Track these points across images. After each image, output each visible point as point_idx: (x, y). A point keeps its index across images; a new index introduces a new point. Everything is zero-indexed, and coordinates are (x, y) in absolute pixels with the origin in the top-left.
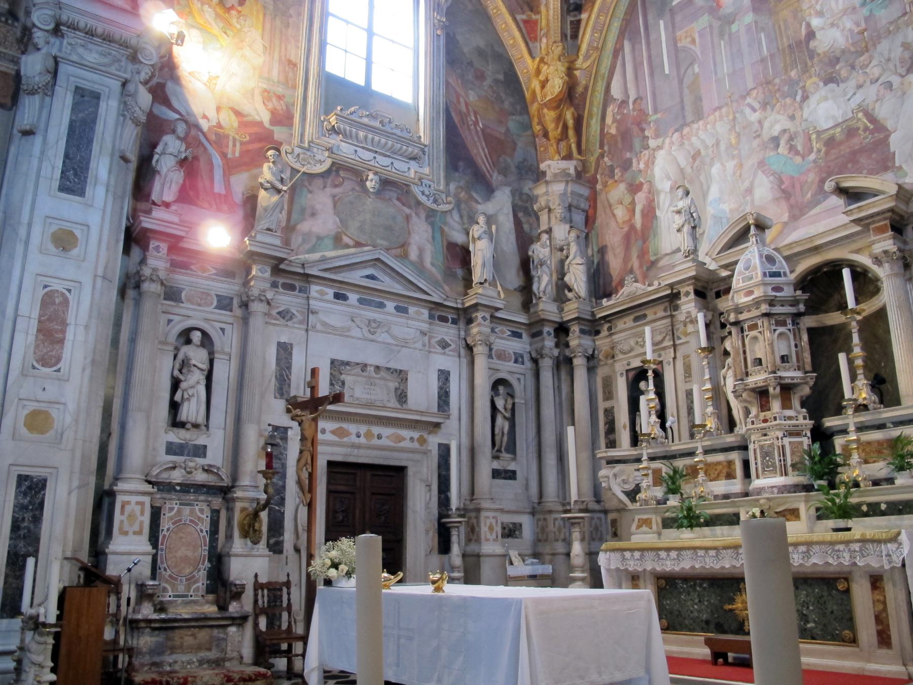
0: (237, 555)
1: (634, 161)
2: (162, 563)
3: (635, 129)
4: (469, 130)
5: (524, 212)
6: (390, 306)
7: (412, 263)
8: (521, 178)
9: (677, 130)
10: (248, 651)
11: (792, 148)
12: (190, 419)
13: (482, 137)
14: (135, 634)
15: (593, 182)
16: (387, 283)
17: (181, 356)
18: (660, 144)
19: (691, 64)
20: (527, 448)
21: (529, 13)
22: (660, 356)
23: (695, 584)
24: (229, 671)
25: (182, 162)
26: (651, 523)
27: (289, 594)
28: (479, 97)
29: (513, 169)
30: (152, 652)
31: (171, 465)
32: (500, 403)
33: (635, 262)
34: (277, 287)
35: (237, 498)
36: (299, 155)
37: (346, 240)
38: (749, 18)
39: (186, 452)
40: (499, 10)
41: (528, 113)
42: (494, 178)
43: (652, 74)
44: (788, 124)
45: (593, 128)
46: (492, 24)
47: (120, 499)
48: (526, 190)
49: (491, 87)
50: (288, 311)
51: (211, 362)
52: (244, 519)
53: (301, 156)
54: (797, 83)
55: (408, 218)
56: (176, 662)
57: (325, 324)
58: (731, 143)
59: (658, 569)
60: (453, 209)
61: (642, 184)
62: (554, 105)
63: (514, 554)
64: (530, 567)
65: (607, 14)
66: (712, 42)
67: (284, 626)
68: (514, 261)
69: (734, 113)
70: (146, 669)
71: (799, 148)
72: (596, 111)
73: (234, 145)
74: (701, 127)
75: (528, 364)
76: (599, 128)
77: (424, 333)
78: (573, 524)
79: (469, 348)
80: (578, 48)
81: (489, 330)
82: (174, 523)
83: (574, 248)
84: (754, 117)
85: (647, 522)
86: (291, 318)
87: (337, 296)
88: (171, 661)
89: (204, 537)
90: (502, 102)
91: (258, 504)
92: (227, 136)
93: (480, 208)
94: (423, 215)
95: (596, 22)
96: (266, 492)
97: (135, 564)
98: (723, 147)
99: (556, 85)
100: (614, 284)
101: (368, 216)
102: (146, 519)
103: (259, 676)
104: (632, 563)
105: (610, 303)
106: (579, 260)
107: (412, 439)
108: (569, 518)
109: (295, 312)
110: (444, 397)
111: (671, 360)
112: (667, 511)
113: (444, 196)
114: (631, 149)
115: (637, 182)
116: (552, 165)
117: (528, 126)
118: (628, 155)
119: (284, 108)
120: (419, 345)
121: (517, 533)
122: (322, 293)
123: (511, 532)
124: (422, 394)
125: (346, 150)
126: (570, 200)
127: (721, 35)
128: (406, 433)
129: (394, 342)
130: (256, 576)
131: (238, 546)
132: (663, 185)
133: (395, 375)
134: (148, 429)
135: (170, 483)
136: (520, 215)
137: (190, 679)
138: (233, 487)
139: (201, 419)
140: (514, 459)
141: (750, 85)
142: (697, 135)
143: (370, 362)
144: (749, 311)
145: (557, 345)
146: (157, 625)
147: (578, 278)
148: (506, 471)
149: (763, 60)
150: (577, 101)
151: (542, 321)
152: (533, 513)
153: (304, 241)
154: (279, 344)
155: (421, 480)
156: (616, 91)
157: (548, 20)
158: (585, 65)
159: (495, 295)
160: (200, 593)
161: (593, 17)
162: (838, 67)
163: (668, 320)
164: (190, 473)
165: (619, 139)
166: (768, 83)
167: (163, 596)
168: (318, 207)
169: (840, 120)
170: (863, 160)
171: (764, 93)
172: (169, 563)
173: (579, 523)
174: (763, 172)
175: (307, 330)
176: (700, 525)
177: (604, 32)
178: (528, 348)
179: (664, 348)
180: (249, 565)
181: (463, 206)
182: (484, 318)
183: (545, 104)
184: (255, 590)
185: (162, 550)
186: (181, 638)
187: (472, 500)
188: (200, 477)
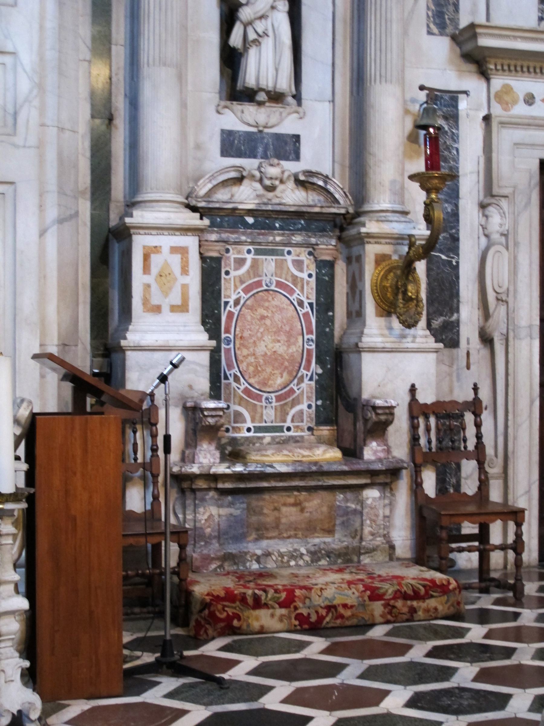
0: (373, 350)
2: (230, 366)
10: (402, 535)
12: (263, 84)
14: (189, 502)
24: (371, 576)
27: (478, 425)
30: (221, 535)
31: (233, 174)
35: (369, 235)
39: (260, 150)
52: (385, 277)
67: (470, 487)
70: (213, 566)
82: (246, 290)
88: (259, 552)
89: (306, 315)
91: (411, 245)
97: (175, 366)
102: (193, 281)
103: (432, 588)
130: (413, 390)
131: (375, 331)
134: (183, 105)
135: (235, 209)
138: (358, 214)
146: (228, 485)
160: (305, 425)
167: (238, 430)
180: (397, 368)
184: (413, 417)
185: (228, 342)
186: (275, 509)
188: (292, 197)
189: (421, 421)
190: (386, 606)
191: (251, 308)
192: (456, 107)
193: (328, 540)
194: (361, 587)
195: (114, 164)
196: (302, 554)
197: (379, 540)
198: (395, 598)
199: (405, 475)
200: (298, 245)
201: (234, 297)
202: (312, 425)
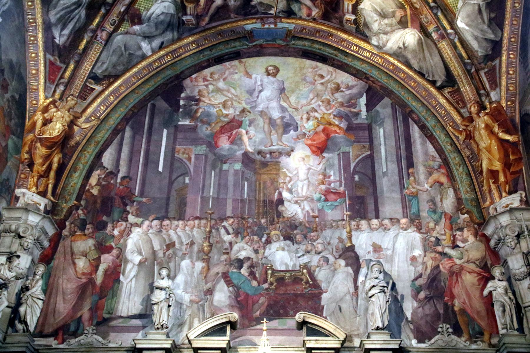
1: (110, 226)
3: (118, 201)
9: (157, 218)
11: (252, 274)
18: (139, 223)
38: (238, 166)
44: (253, 255)
45: (76, 180)
54: (265, 229)
61: (112, 248)
62: (48, 144)
65: (117, 97)
66: (205, 168)
69: (211, 228)
71: (257, 275)
74: (180, 226)
84: (227, 238)
98: (196, 248)
99: (56, 129)
115: (107, 244)
118: (104, 218)
141: (229, 213)
142: (175, 230)
149: (243, 201)
150: (66, 151)
161: (107, 93)
162: (295, 232)
165: (99, 201)
166: (243, 218)
169: (290, 268)
170: (302, 303)
171: (238, 224)
174: (226, 282)
177: (109, 109)
183: (40, 140)
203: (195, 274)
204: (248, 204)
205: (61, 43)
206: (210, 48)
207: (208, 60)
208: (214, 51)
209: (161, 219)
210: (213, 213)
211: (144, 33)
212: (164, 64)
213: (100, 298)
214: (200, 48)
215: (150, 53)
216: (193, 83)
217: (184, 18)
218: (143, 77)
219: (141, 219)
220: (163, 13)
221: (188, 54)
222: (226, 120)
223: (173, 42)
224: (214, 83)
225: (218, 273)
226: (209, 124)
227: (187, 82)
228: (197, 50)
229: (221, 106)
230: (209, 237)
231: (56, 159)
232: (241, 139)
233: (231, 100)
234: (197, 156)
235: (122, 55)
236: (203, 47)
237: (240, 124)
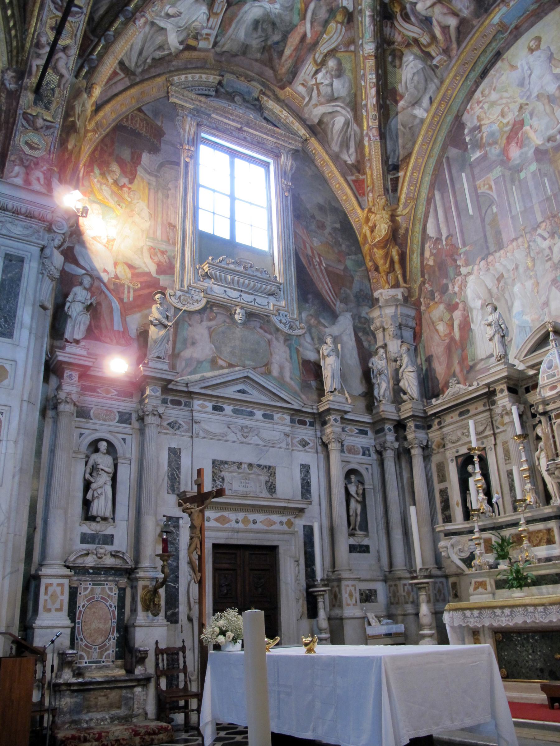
0: (140, 626)
1: (450, 286)
2: (79, 634)
3: (449, 261)
4: (315, 269)
5: (363, 331)
6: (259, 414)
7: (275, 378)
8: (359, 305)
9: (483, 259)
10: (151, 708)
12: (99, 514)
13: (325, 274)
15: (417, 305)
16: (255, 396)
17: (91, 462)
18: (470, 271)
19: (490, 206)
20: (377, 526)
21: (357, 174)
22: (483, 443)
23: (528, 637)
24: (136, 726)
25: (89, 308)
26: (485, 584)
27: (184, 657)
28: (321, 242)
29: (352, 297)
30: (71, 712)
31: (85, 552)
32: (352, 489)
33: (457, 368)
34: (166, 403)
35: (140, 578)
36: (180, 297)
37: (220, 362)
38: (533, 167)
39: (97, 541)
40: (333, 174)
41: (361, 252)
42: (337, 306)
43: (459, 216)
45: (415, 261)
46: (328, 184)
47: (44, 582)
48: (363, 314)
49: (330, 234)
50: (176, 422)
51: (116, 466)
52: (146, 595)
53: (182, 297)
55: (269, 342)
56: (91, 720)
57: (206, 431)
58: (528, 267)
59: (495, 624)
60: (306, 333)
61: (457, 304)
62: (382, 245)
63: (371, 616)
64: (385, 627)
65: (419, 171)
66: (506, 186)
67: (181, 686)
68: (358, 372)
69: (528, 242)
70: (66, 726)
72: (416, 247)
73: (129, 292)
75: (374, 456)
76: (419, 262)
77: (287, 435)
78: (420, 588)
79: (325, 445)
80: (398, 199)
81: (340, 430)
82: (88, 601)
83: (405, 359)
84: (545, 244)
85: (482, 584)
86: (179, 428)
87: (215, 408)
88: (87, 719)
89: (113, 611)
90: (341, 245)
91: (157, 582)
92: (123, 285)
93: (327, 330)
94: (282, 339)
95: (411, 178)
96: (163, 572)
97: (58, 636)
98: (521, 270)
100: (440, 386)
101: (237, 343)
103: (161, 730)
104: (472, 620)
105: (439, 402)
106: (410, 369)
107: (281, 522)
108: (416, 584)
109: (182, 423)
110: (306, 486)
111: (493, 446)
112: (499, 574)
113: (297, 323)
114: (447, 276)
115: (454, 302)
116: (384, 293)
117: (363, 263)
118: (445, 281)
119: (167, 260)
120: (283, 445)
121: (373, 598)
122: (203, 406)
123: (368, 597)
124: (288, 485)
125: (218, 290)
126: (400, 320)
127: (513, 181)
128: (276, 518)
129: (263, 443)
130: (157, 643)
131: (141, 618)
132: (475, 303)
133: (265, 470)
134: (66, 523)
135: (85, 567)
136: (360, 334)
137: (103, 734)
138: (136, 568)
139: (108, 513)
140: (367, 536)
141: (540, 219)
143: (244, 460)
144: (554, 402)
145: (397, 439)
146: (75, 688)
147: (410, 383)
148: (361, 546)
149: (548, 199)
150: (400, 241)
151: (384, 420)
152: (385, 580)
153: (187, 365)
154: (170, 449)
155: (291, 557)
156: (431, 231)
157: (372, 179)
158: (405, 212)
159: (344, 400)
160: (111, 659)
161: (408, 174)
163: (488, 413)
164: (100, 558)
165: (436, 269)
167: (80, 663)
168: (197, 337)
171: (551, 224)
172: (85, 634)
173: (425, 588)
174: (557, 288)
175: (192, 437)
176: (528, 585)
177: (418, 185)
178: (373, 443)
179: (486, 437)
180: (151, 634)
181: (313, 330)
182: (335, 420)
183: (375, 245)
184: (157, 655)
185: (79, 624)
186: (96, 698)
187: (334, 572)
189: (160, 656)
190: (141, 738)
191: (90, 609)
192: (178, 522)
193: (118, 711)
194: (131, 731)
195: (35, 547)
196: (106, 719)
197: (141, 711)
198: (145, 735)
199: (153, 681)
200: (111, 581)
201: (82, 604)
202: (114, 660)
203: (528, 295)
204: (555, 199)
205: (353, 161)
206: (472, 69)
207: (475, 81)
208: (477, 69)
209: (485, 258)
210: (525, 227)
211: (410, 102)
212: (442, 114)
213: (463, 351)
214: (465, 76)
215: (425, 115)
216: (470, 113)
217: (435, 62)
218: (431, 139)
219: (471, 267)
220: (414, 74)
221: (457, 89)
222: (509, 128)
223: (438, 89)
224: (487, 100)
225: (548, 283)
226: (496, 143)
227: (466, 118)
228: (463, 79)
229: (500, 117)
230: (530, 252)
231: (395, 253)
232: (528, 138)
233: (507, 104)
234: (496, 181)
235: (404, 134)
236: (467, 73)
237: (522, 123)
